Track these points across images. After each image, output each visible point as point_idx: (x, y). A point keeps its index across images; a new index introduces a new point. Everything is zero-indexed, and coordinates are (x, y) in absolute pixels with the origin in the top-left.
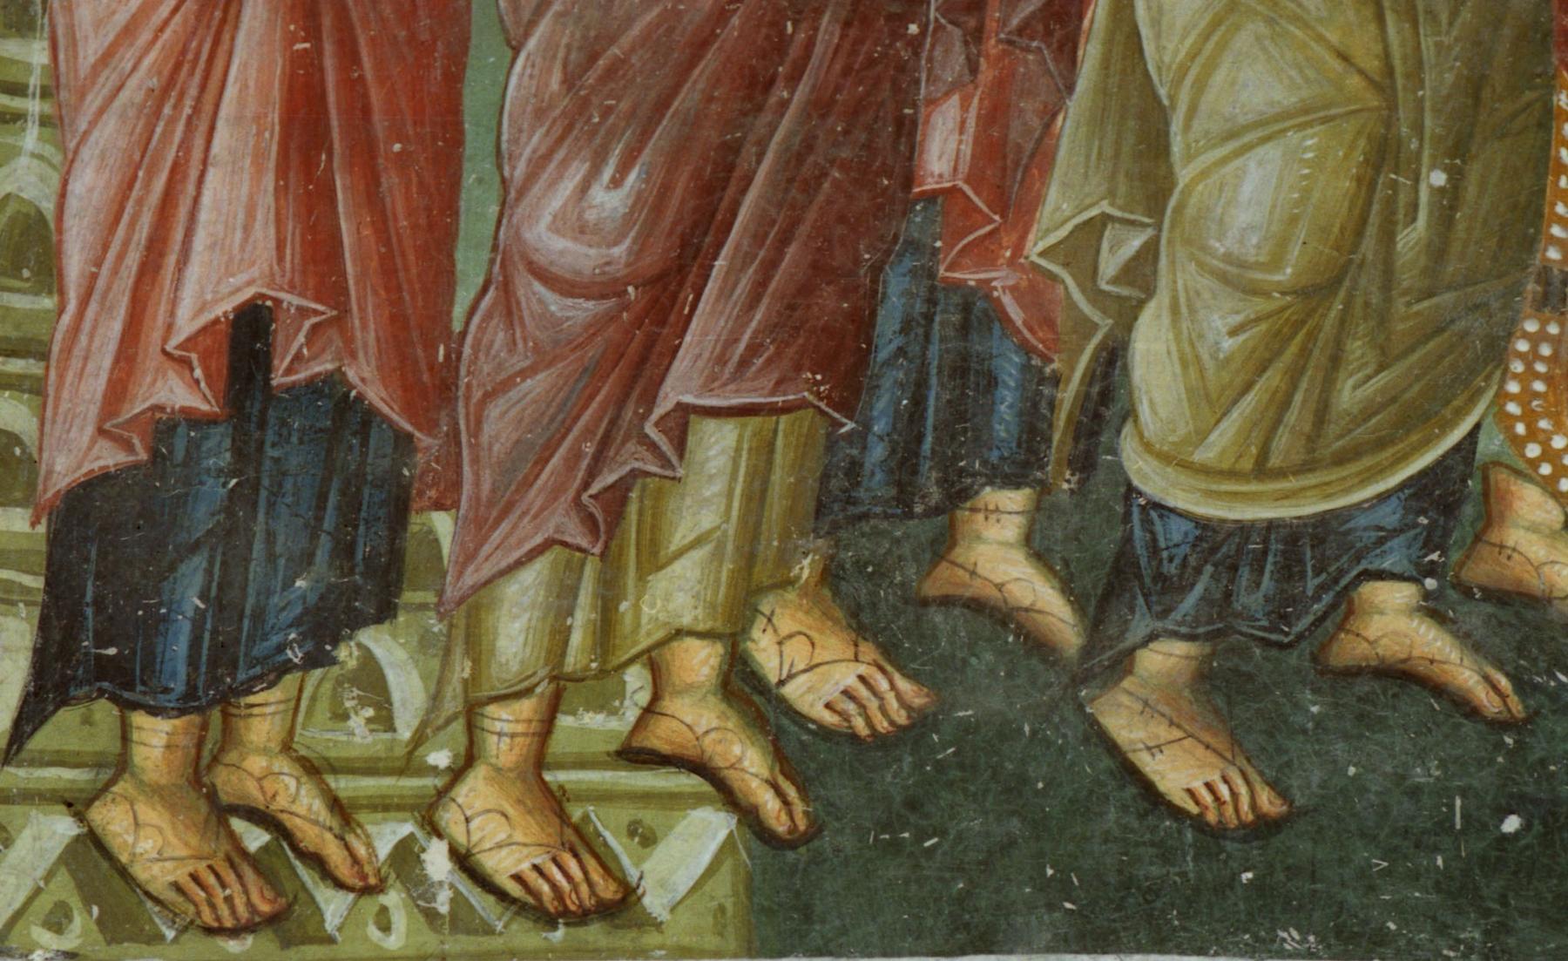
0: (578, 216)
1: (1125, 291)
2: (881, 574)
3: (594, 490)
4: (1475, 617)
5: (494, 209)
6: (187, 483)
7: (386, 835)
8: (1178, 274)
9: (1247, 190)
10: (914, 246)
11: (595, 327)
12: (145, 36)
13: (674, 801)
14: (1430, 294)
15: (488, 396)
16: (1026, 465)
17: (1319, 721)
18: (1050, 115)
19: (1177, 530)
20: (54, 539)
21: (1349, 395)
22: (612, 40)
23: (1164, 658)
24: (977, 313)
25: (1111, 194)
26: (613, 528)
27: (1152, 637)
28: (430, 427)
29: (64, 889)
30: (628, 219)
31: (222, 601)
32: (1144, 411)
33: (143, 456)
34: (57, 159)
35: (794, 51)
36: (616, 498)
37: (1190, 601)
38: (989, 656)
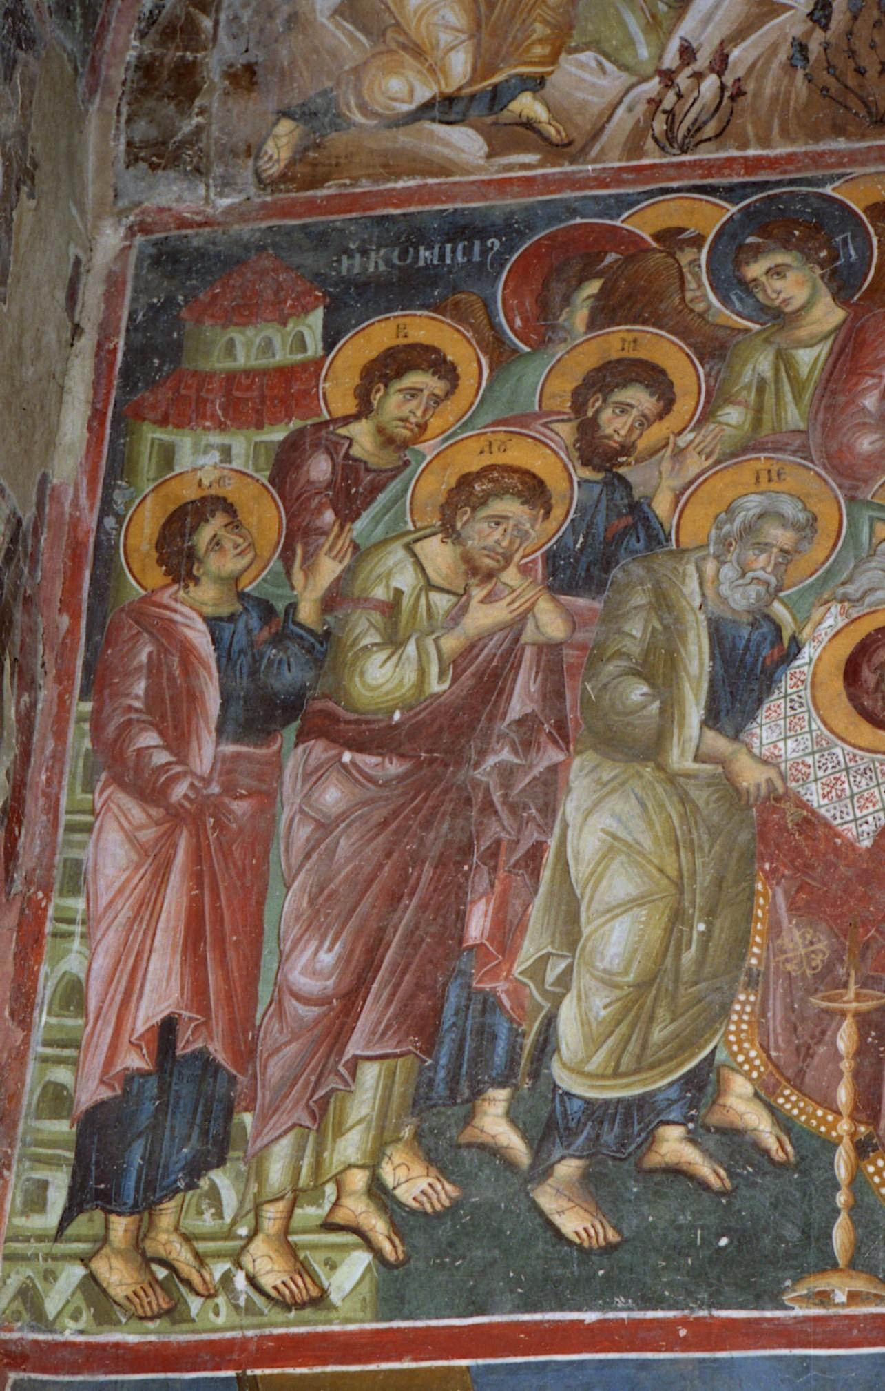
0: (311, 965)
1: (557, 990)
2: (441, 1133)
3: (316, 1097)
4: (711, 1141)
5: (275, 965)
6: (137, 1104)
7: (219, 1269)
8: (582, 980)
9: (614, 938)
10: (462, 973)
11: (317, 1021)
12: (127, 893)
13: (345, 1248)
14: (696, 984)
15: (270, 1056)
16: (508, 1077)
17: (637, 1195)
18: (526, 906)
19: (576, 1105)
20: (80, 1134)
21: (657, 1035)
22: (331, 880)
23: (568, 1168)
24: (490, 1004)
25: (552, 943)
26: (323, 1116)
27: (563, 1158)
28: (243, 1071)
29: (79, 1301)
30: (335, 966)
31: (150, 1161)
32: (563, 1047)
33: (119, 1092)
34: (87, 952)
35: (412, 881)
36: (324, 1102)
37: (582, 1138)
38: (487, 1171)
